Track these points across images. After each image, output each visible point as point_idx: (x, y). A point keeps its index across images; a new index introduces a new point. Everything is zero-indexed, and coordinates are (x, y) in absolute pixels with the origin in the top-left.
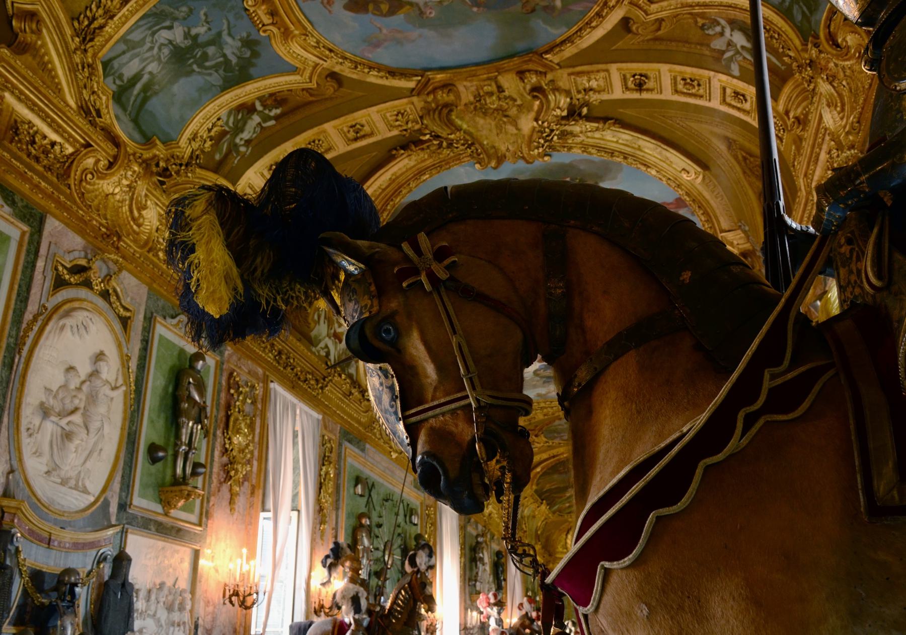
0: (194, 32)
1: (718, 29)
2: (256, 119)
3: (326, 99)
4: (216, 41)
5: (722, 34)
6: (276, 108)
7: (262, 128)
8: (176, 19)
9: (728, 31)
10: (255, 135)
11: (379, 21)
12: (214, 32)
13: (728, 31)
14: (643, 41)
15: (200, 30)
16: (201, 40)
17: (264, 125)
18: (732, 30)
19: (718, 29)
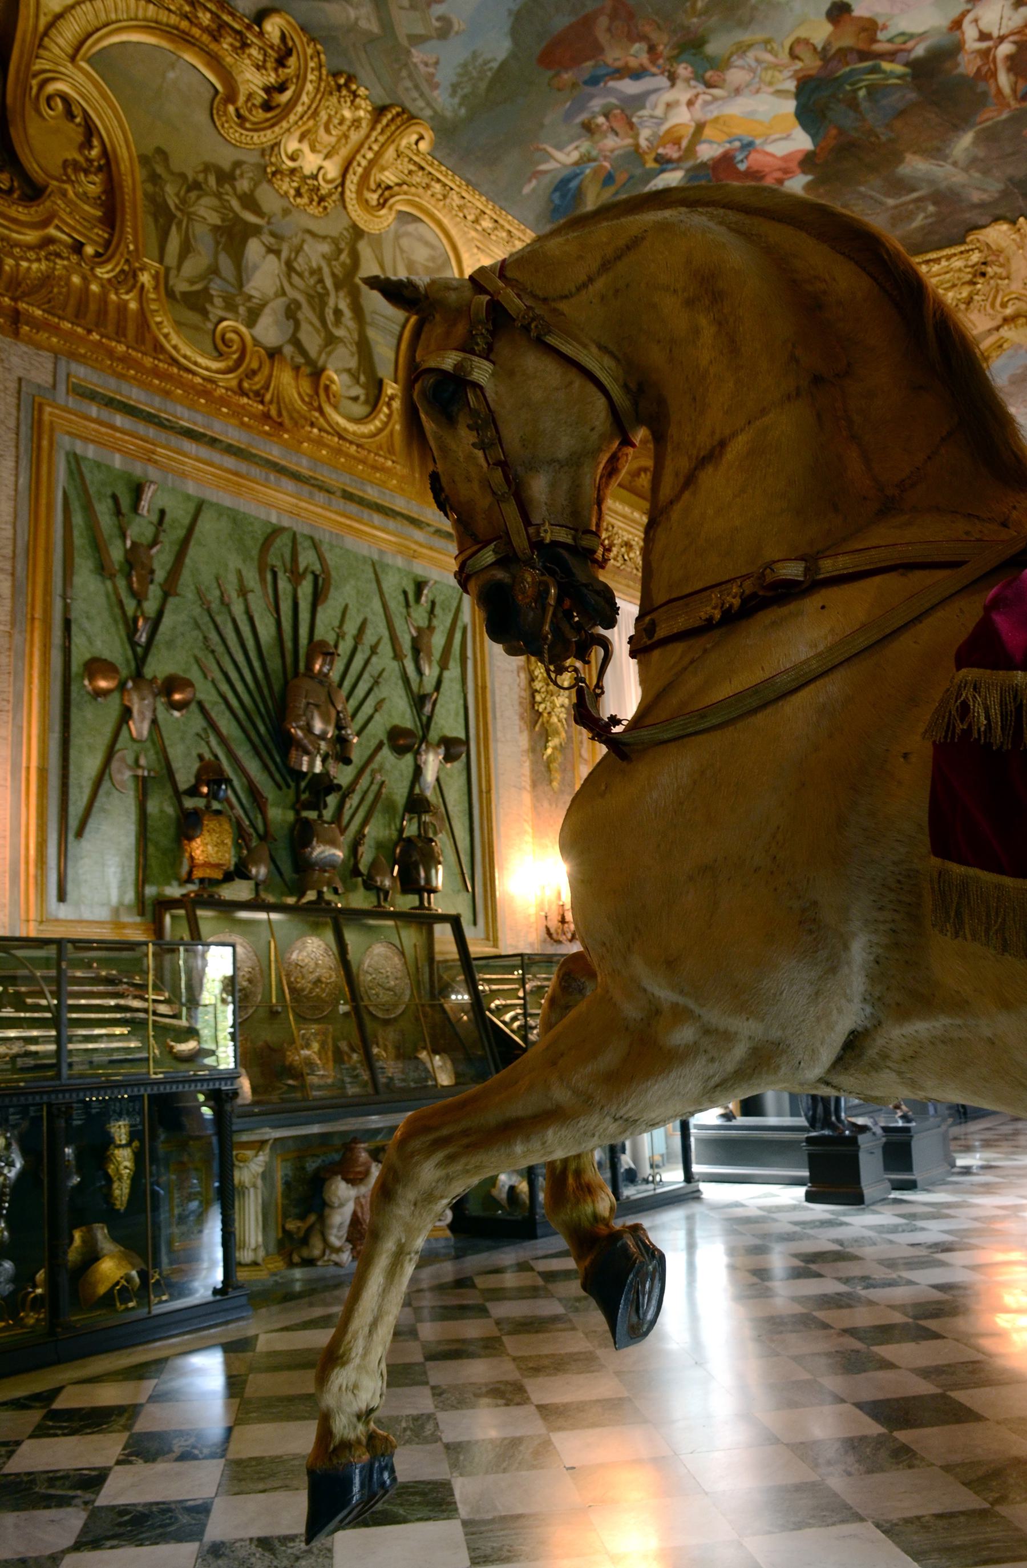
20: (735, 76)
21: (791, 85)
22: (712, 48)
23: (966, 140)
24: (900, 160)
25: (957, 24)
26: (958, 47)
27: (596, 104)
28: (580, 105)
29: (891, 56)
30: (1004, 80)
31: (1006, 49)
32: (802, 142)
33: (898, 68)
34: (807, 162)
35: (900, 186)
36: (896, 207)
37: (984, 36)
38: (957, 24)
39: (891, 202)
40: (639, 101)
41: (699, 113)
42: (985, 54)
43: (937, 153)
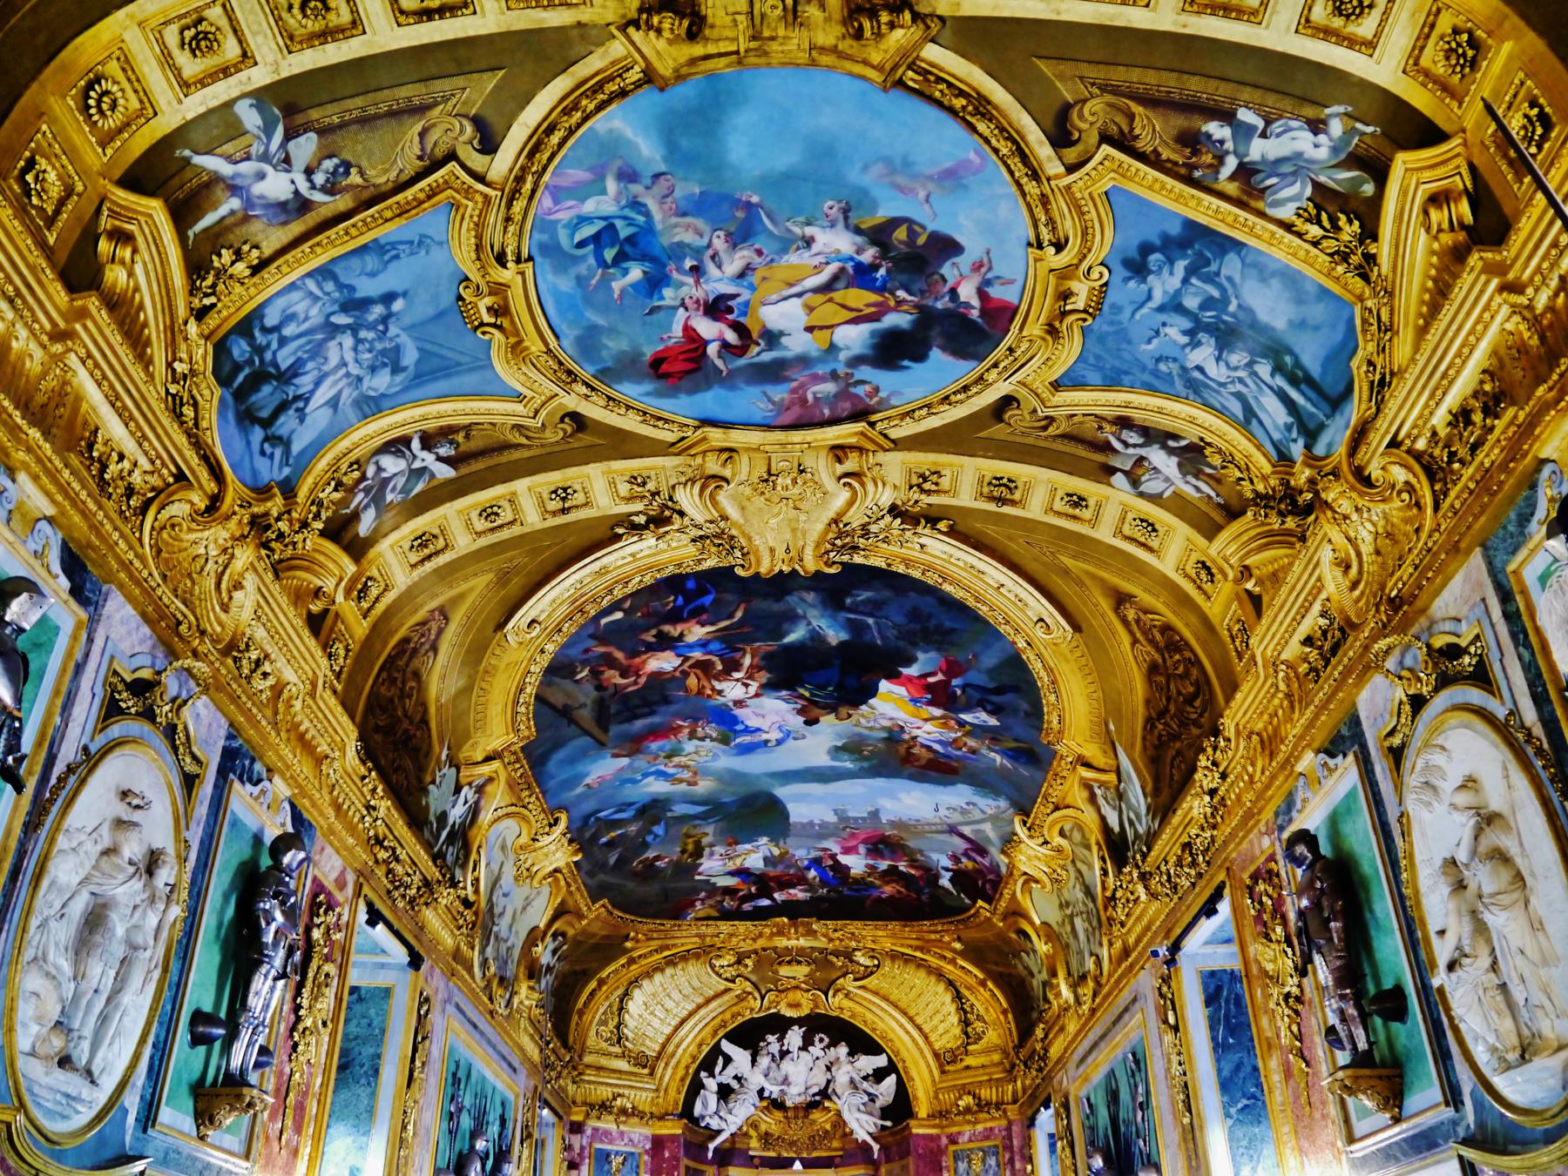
0: (1185, 340)
1: (319, 179)
2: (1258, 149)
3: (1116, 91)
4: (1174, 306)
5: (309, 172)
6: (1209, 136)
7: (1268, 123)
8: (1184, 369)
9: (303, 186)
10: (1294, 124)
11: (920, 214)
12: (1163, 317)
13: (303, 186)
14: (446, 100)
15: (1175, 331)
16: (1187, 324)
17: (1261, 124)
18: (297, 192)
19: (319, 179)
20: (887, 723)
21: (864, 707)
22: (885, 735)
23: (791, 638)
24: (842, 644)
25: (757, 695)
26: (763, 686)
27: (959, 753)
28: (964, 758)
29: (802, 697)
30: (747, 661)
31: (737, 675)
32: (884, 685)
33: (802, 691)
34: (893, 676)
35: (856, 628)
36: (871, 615)
37: (747, 685)
38: (757, 695)
39: (871, 621)
40: (940, 742)
41: (920, 723)
42: (749, 678)
43: (816, 637)
